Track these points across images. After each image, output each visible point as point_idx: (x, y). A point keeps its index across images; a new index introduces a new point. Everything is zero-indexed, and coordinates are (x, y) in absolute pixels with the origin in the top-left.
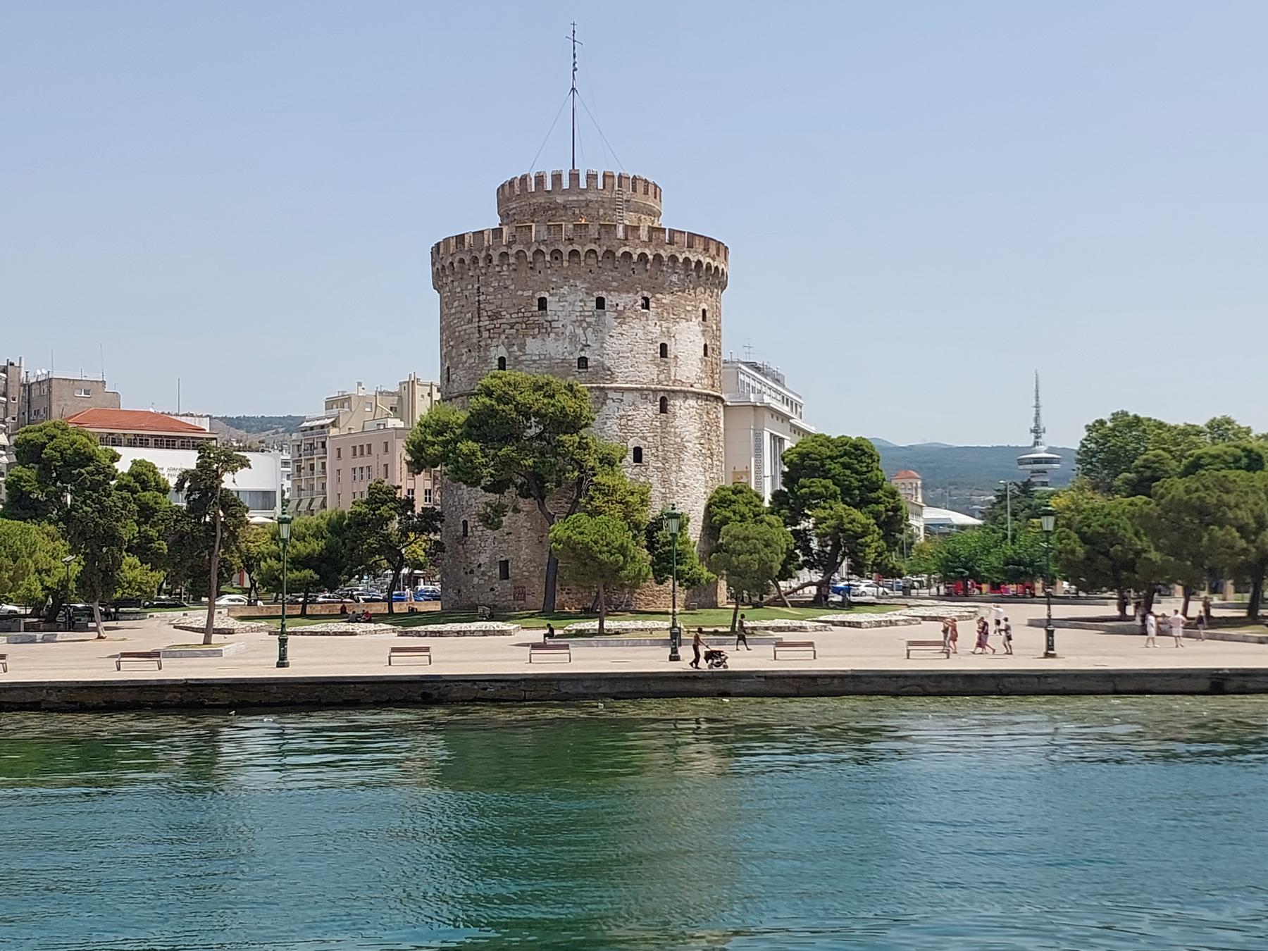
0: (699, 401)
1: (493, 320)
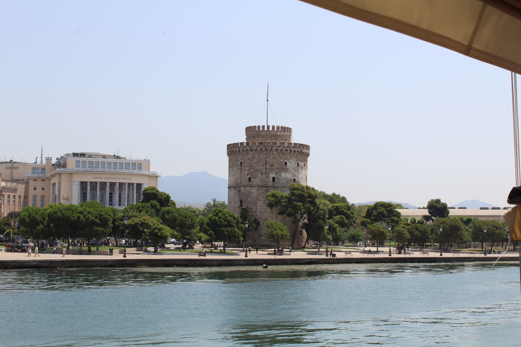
1: (271, 166)
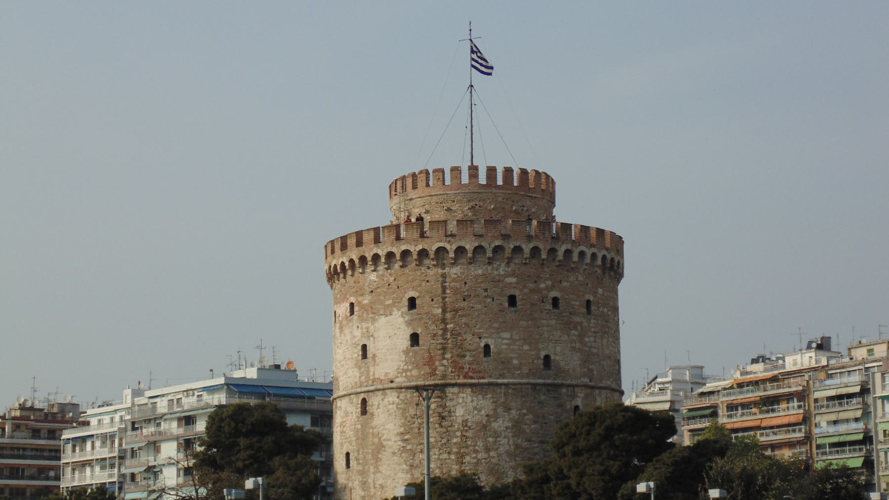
0: (402, 396)
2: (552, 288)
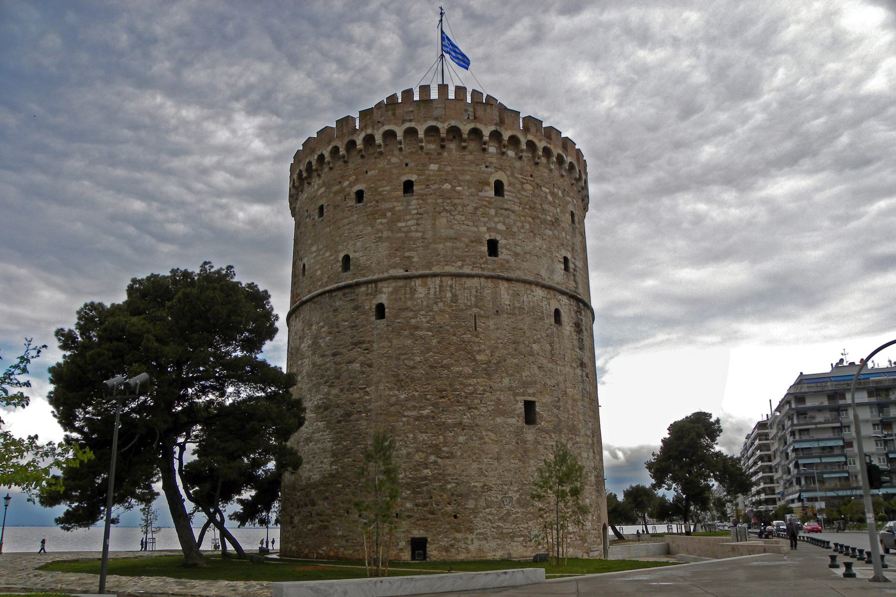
2: (357, 181)
